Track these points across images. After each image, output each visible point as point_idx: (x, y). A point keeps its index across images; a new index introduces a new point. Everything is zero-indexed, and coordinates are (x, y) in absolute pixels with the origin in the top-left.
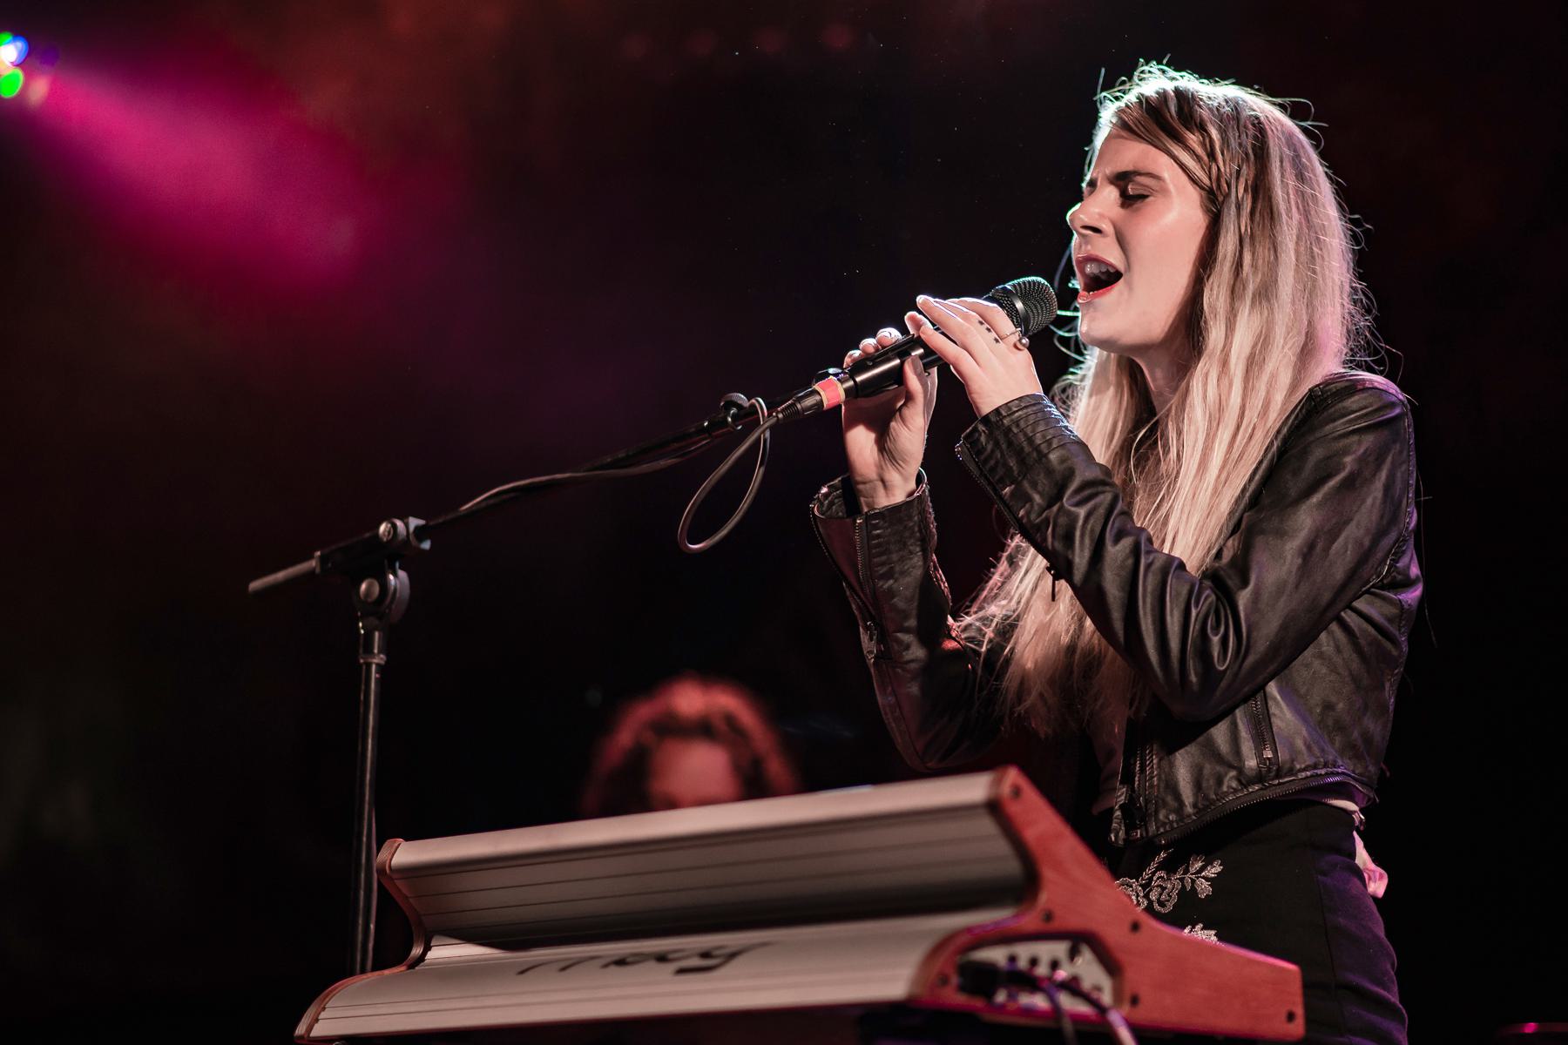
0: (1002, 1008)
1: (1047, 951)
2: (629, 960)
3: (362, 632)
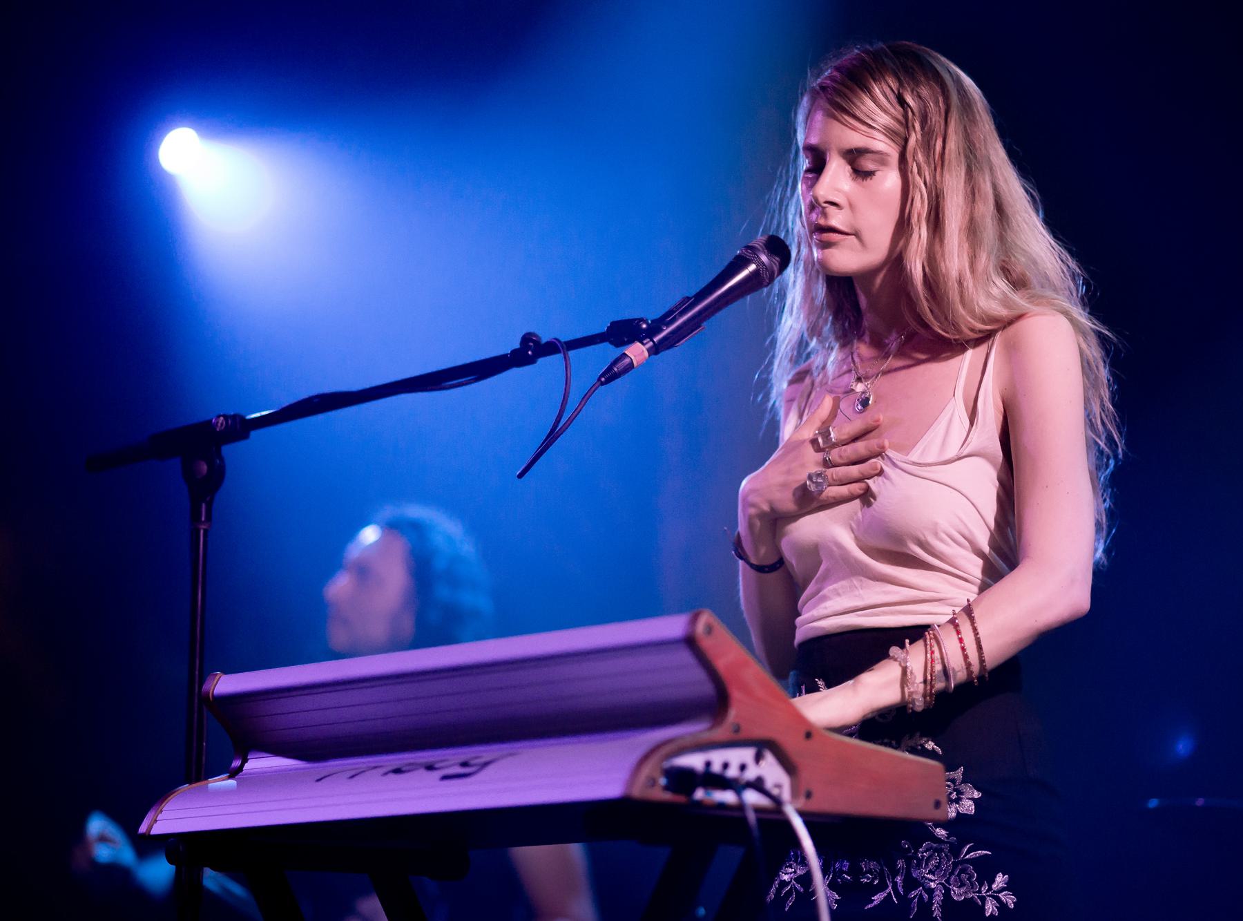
0: (699, 803)
1: (735, 759)
2: (404, 769)
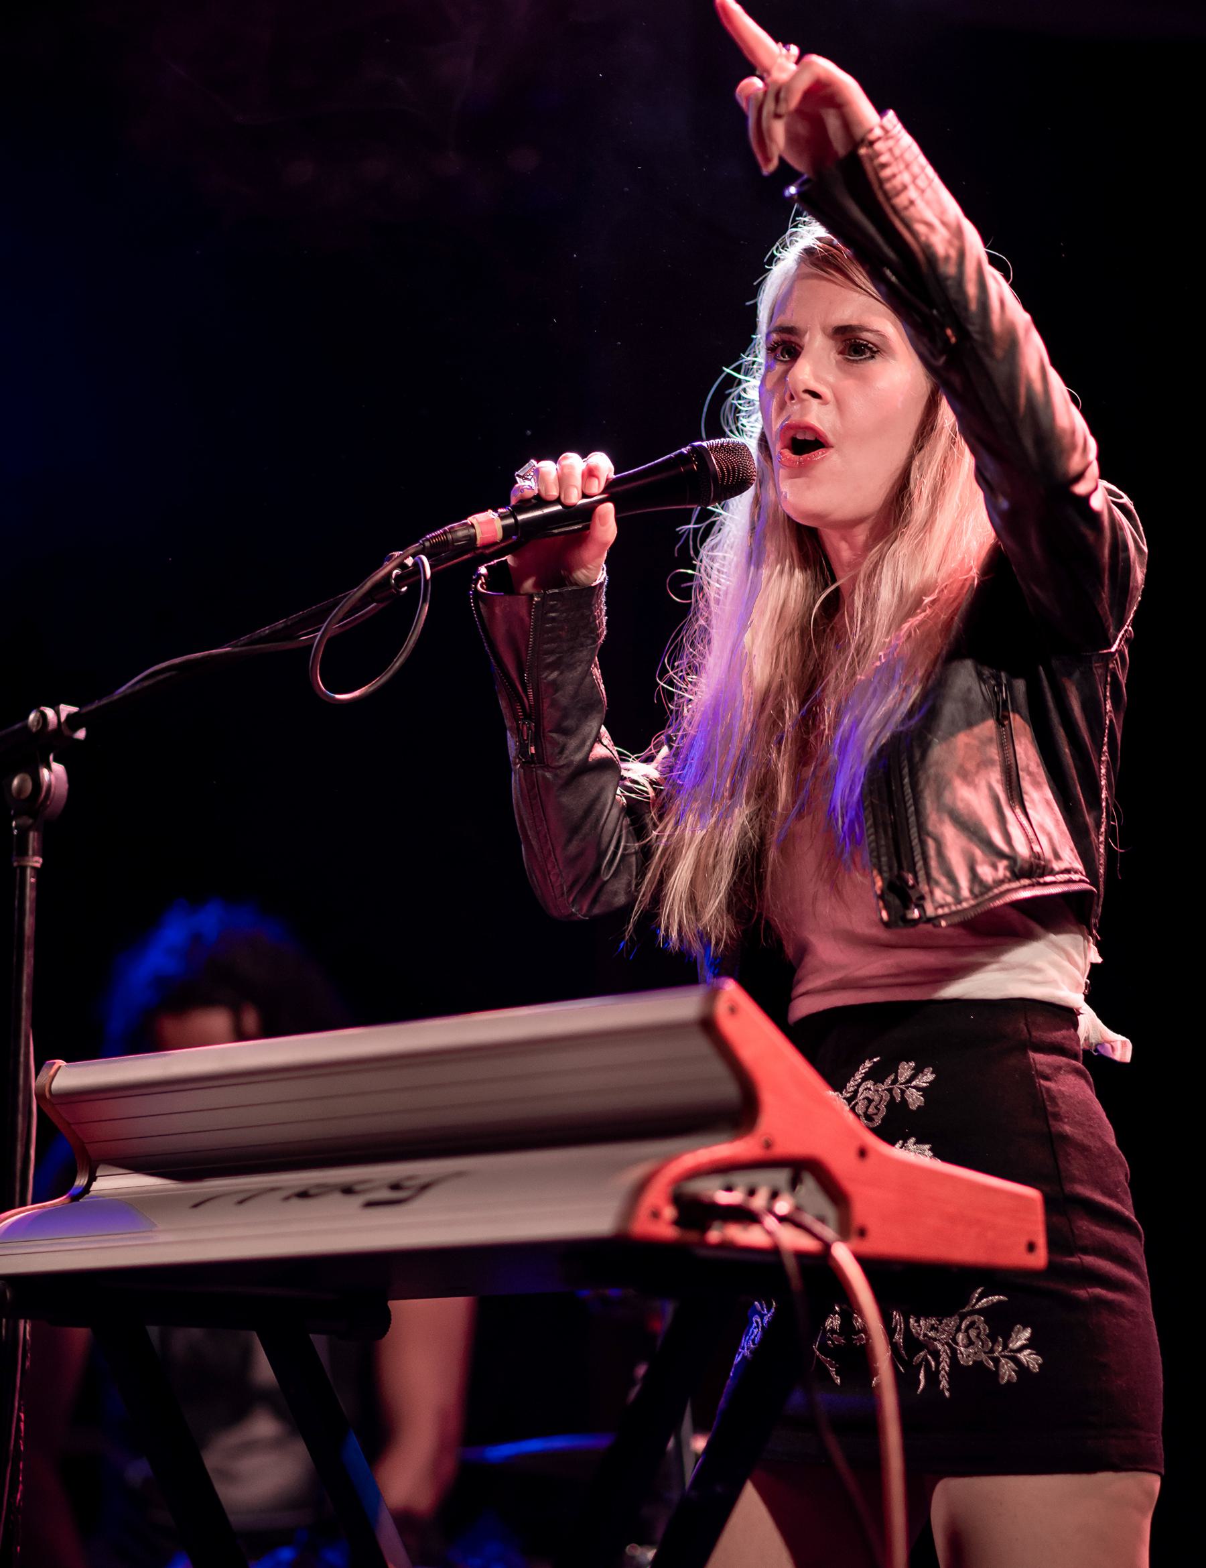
2: (312, 1192)
3: (15, 832)
